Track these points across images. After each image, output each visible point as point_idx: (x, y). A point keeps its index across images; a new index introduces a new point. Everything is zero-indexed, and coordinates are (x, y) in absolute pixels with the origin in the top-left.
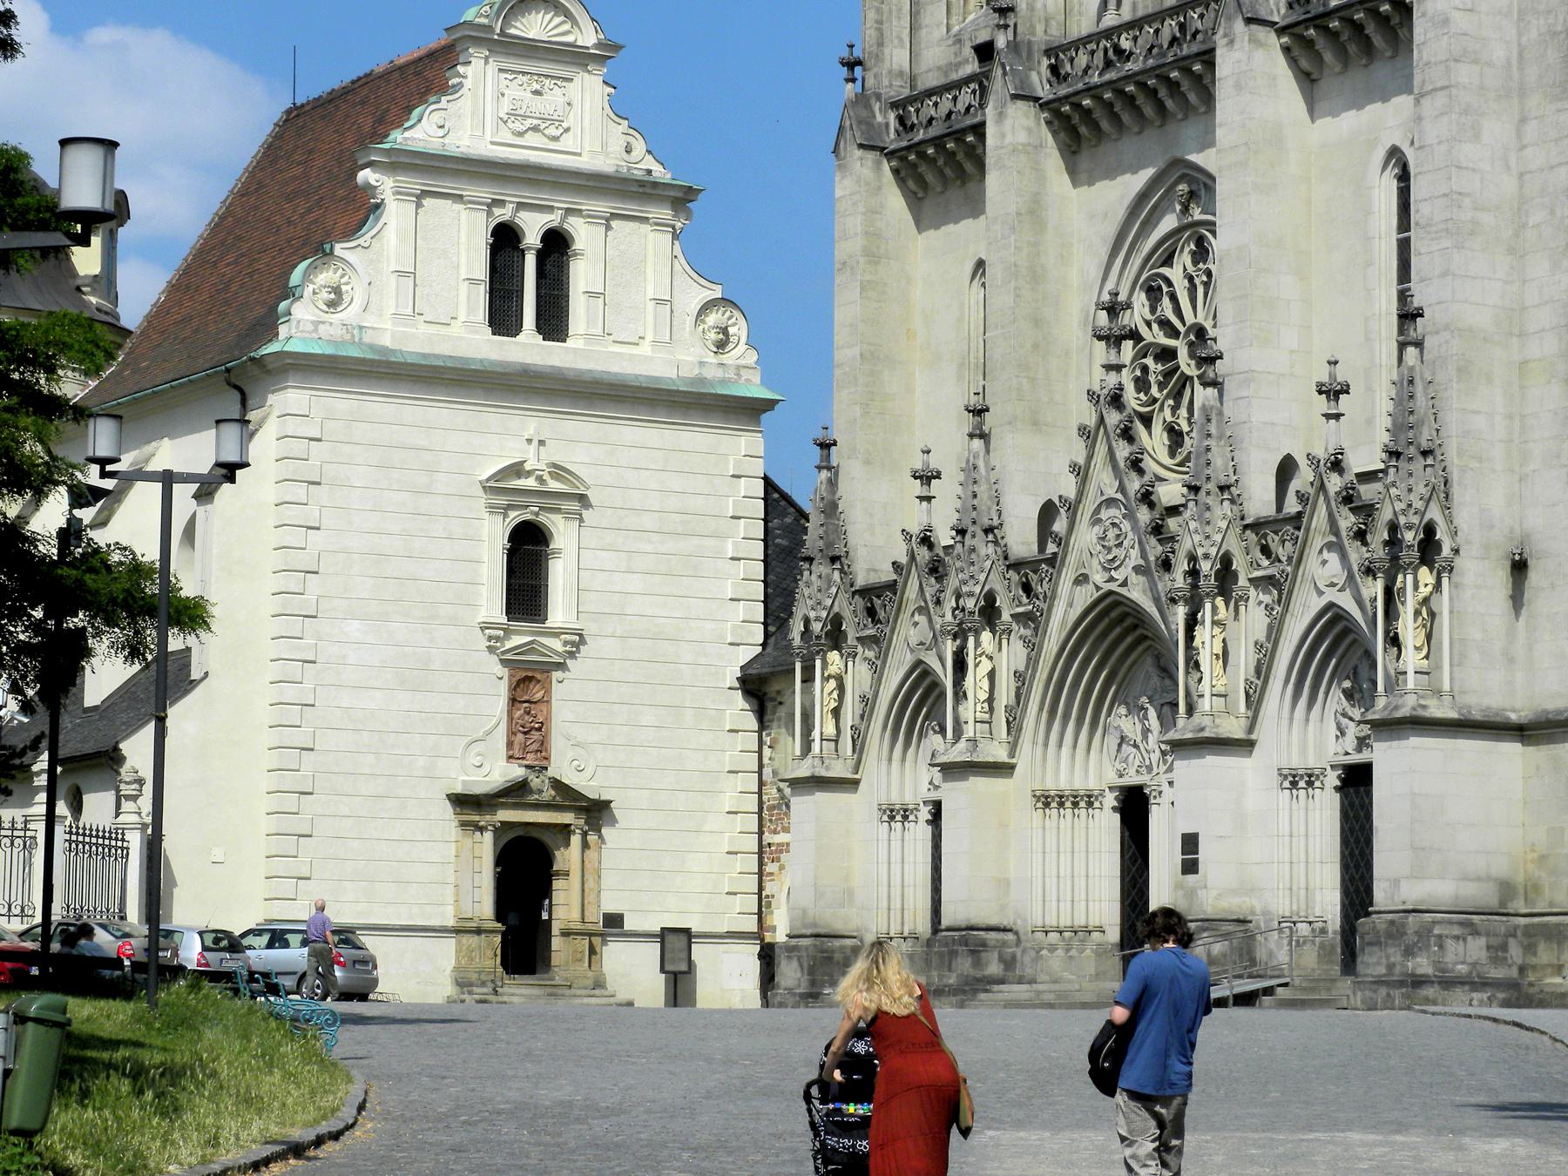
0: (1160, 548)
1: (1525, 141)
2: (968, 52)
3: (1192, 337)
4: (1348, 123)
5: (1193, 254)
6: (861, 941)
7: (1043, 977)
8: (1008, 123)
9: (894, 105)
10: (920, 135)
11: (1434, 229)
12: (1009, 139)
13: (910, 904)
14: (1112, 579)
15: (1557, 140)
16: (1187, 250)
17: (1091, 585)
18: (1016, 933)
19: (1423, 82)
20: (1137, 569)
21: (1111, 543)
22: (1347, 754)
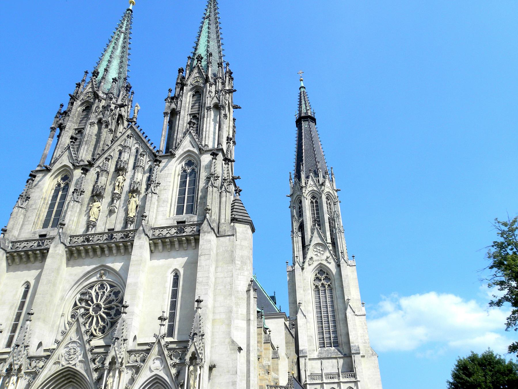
0: (91, 356)
1: (217, 271)
3: (95, 306)
4: (162, 262)
5: (99, 287)
8: (58, 248)
9: (12, 242)
10: (20, 250)
11: (203, 284)
12: (57, 251)
14: (69, 363)
15: (227, 272)
16: (98, 286)
17: (61, 365)
19: (202, 253)
20: (80, 361)
21: (72, 353)
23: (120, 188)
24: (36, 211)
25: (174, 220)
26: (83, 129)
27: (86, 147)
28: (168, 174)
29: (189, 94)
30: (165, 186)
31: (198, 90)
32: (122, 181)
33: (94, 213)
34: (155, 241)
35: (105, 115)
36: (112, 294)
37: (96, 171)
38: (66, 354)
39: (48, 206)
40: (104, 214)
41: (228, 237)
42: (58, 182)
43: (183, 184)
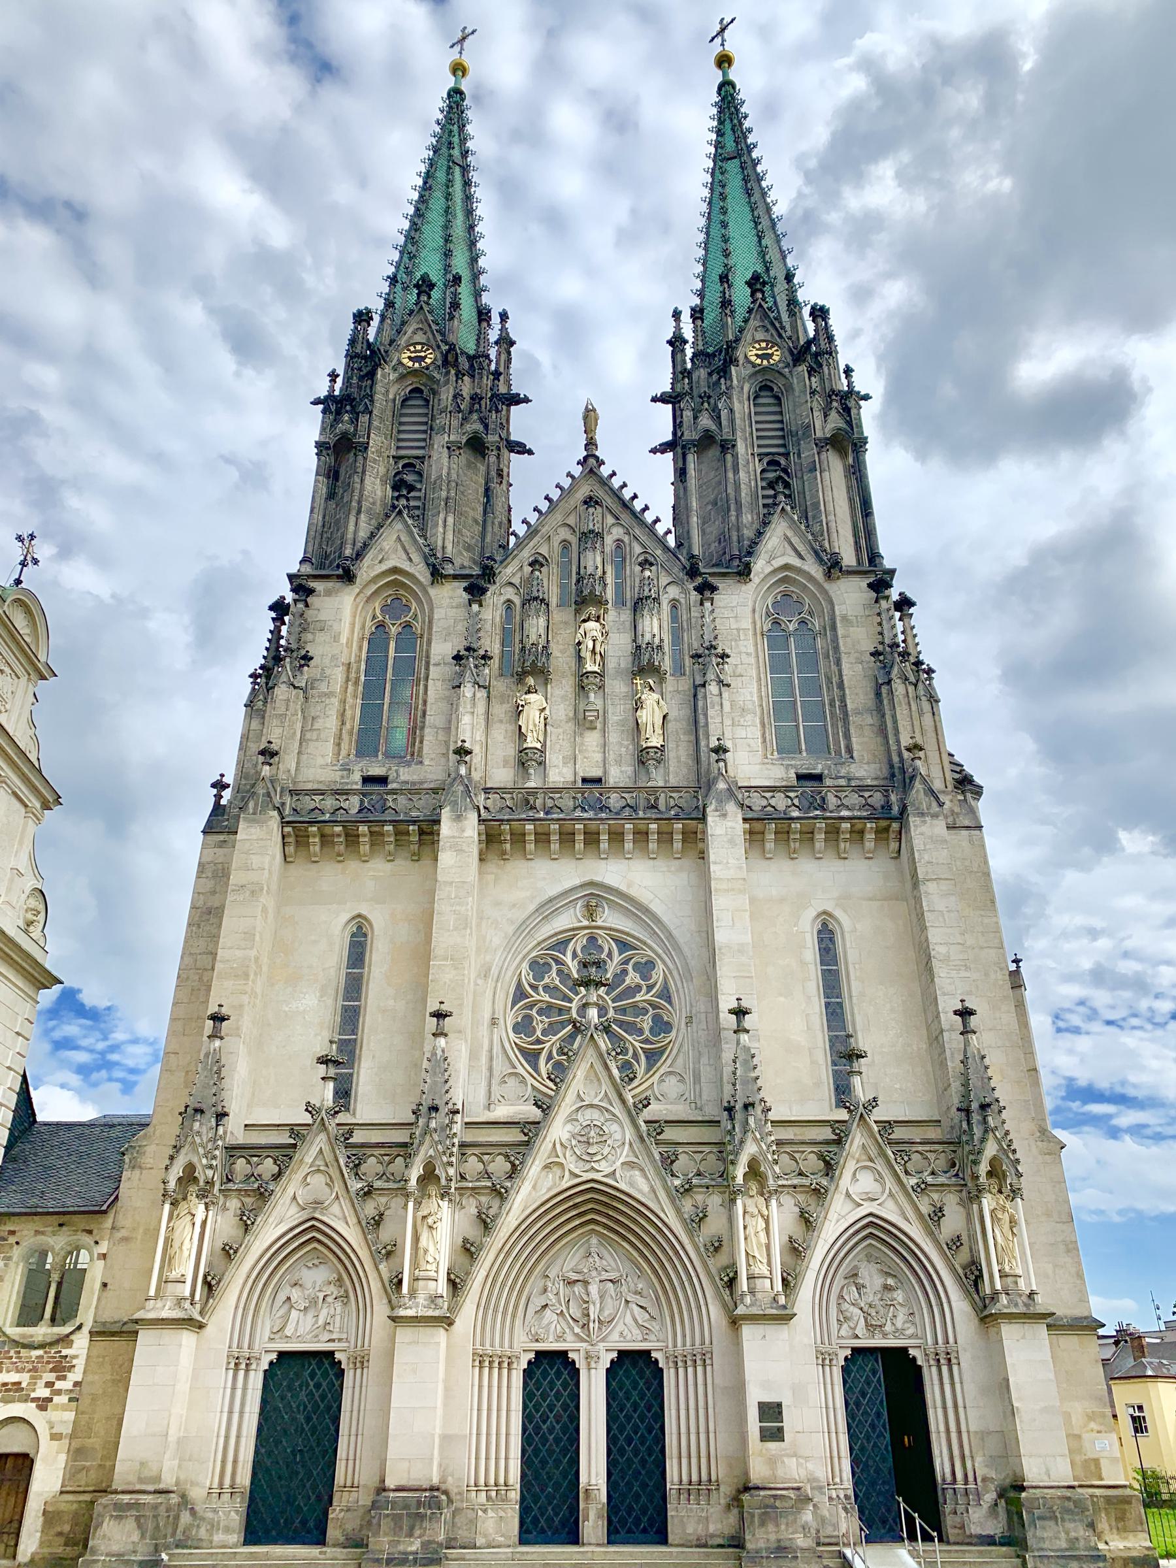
2: (357, 777)
6: (183, 1496)
7: (480, 1541)
9: (292, 792)
10: (327, 817)
13: (241, 1458)
17: (567, 1173)
18: (446, 1493)
22: (857, 1337)
23: (598, 657)
24: (335, 701)
25: (787, 767)
26: (421, 458)
27: (450, 520)
28: (738, 630)
29: (746, 387)
30: (736, 665)
31: (769, 383)
32: (600, 639)
33: (535, 725)
34: (758, 826)
35: (492, 426)
36: (630, 967)
37: (503, 598)
38: (574, 1142)
39: (361, 688)
40: (561, 730)
41: (964, 833)
42: (374, 617)
43: (778, 664)
